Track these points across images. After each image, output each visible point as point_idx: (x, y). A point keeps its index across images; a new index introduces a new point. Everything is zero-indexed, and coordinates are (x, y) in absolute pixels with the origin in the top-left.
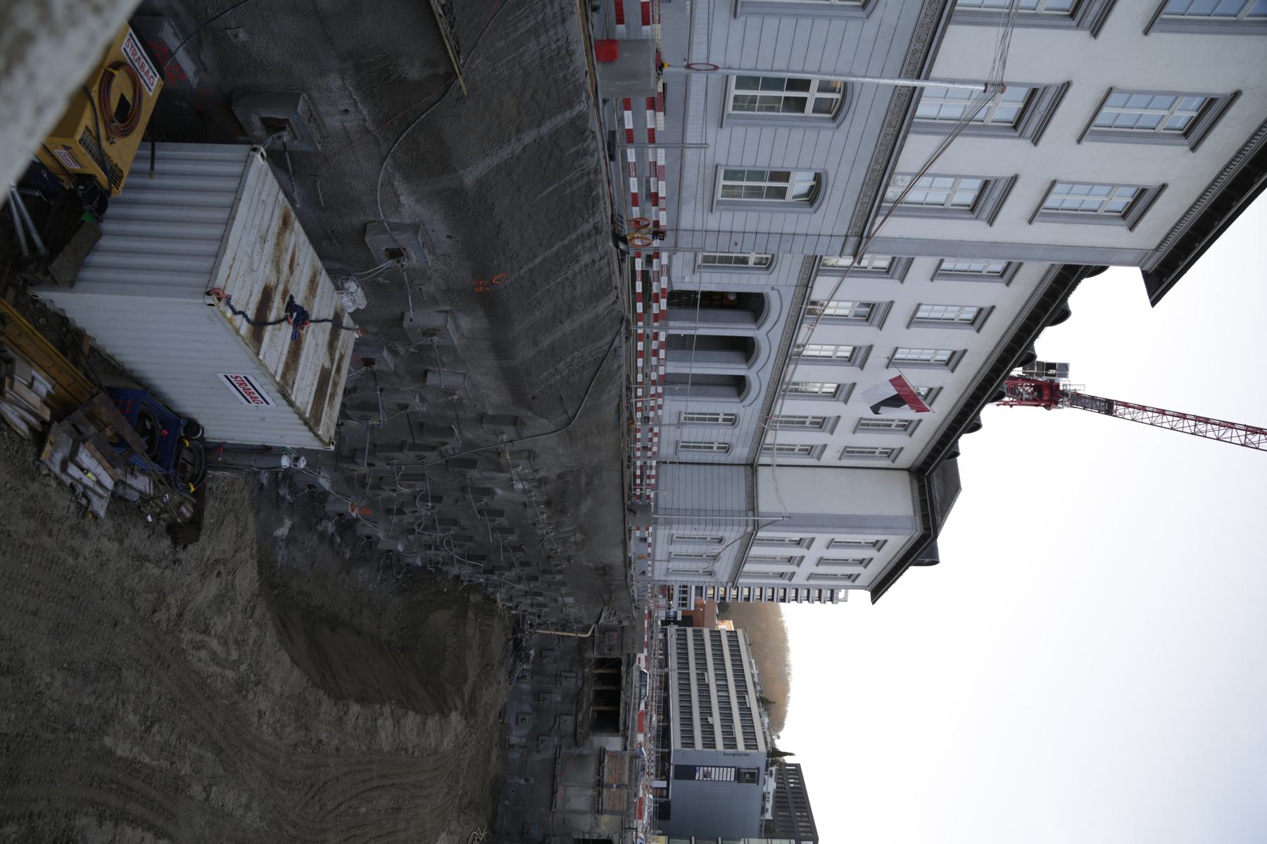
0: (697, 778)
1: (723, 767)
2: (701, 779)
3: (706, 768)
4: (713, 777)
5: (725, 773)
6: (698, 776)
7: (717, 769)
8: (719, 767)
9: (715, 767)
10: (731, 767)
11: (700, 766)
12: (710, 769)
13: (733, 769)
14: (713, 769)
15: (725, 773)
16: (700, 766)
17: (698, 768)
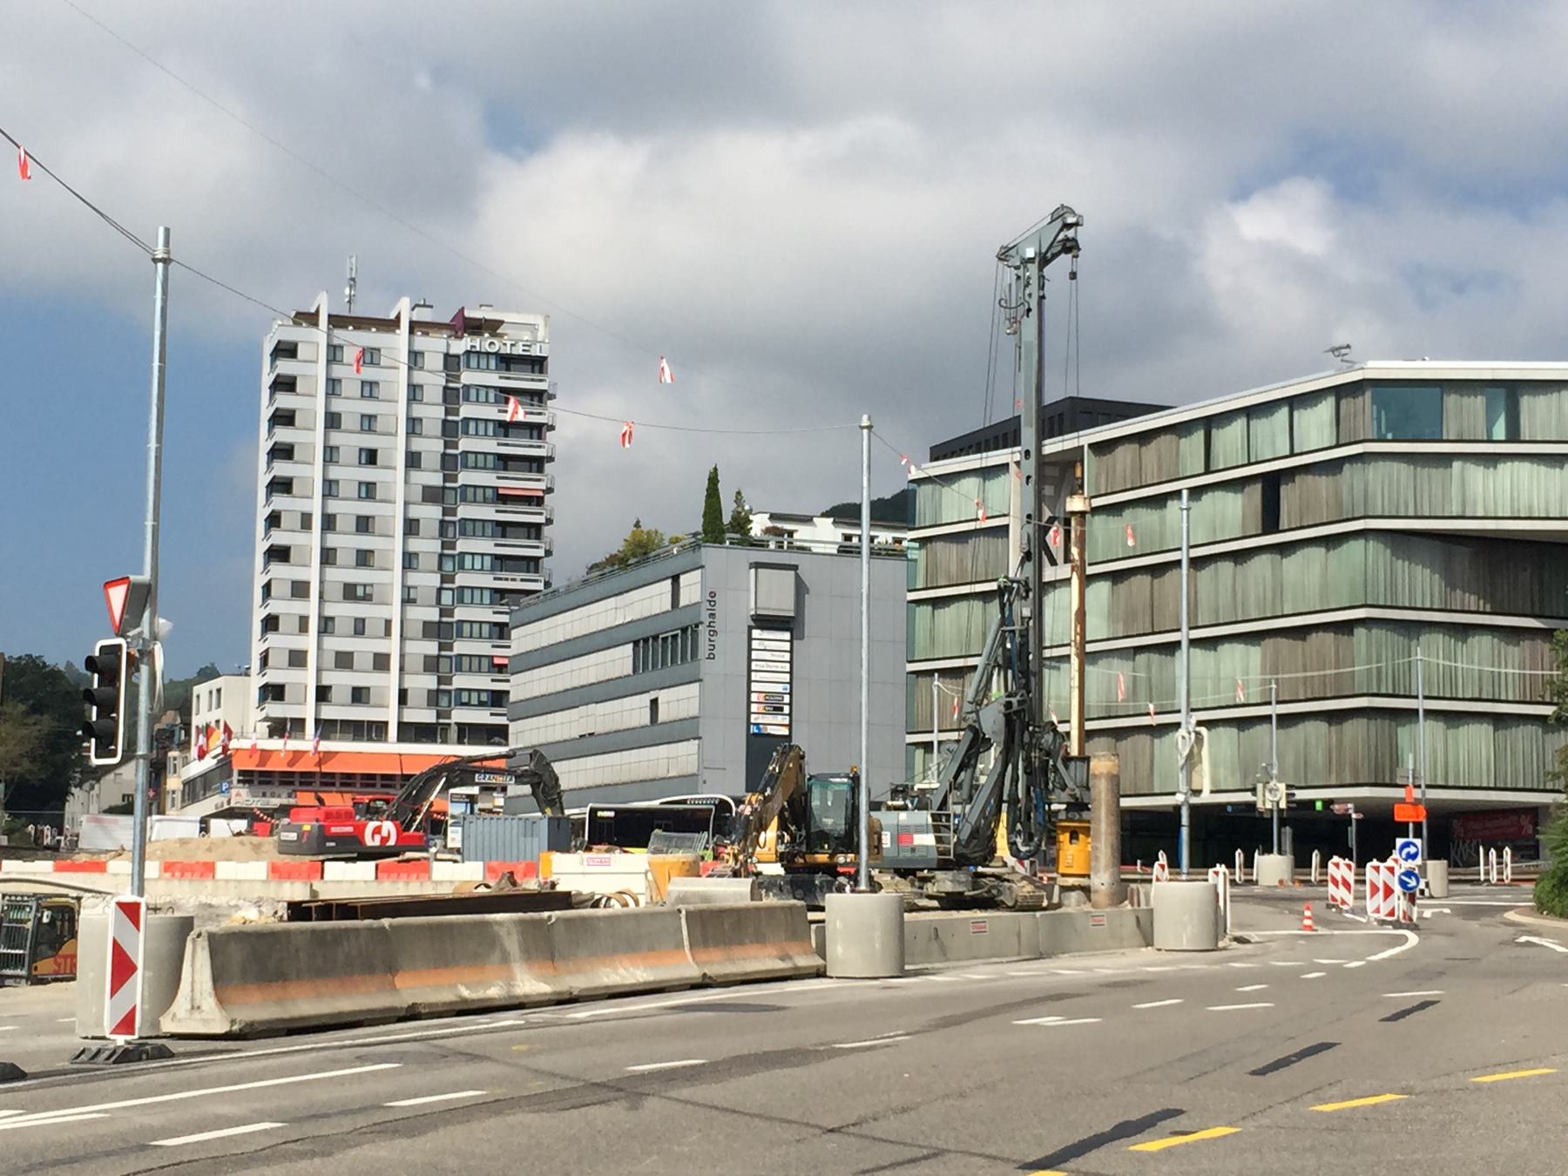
0: (785, 732)
1: (750, 660)
2: (780, 719)
3: (754, 708)
4: (779, 688)
5: (768, 656)
6: (776, 725)
7: (754, 676)
8: (750, 671)
9: (749, 681)
10: (750, 639)
11: (749, 723)
12: (754, 697)
13: (756, 633)
14: (754, 687)
15: (768, 656)
16: (749, 723)
17: (754, 729)
